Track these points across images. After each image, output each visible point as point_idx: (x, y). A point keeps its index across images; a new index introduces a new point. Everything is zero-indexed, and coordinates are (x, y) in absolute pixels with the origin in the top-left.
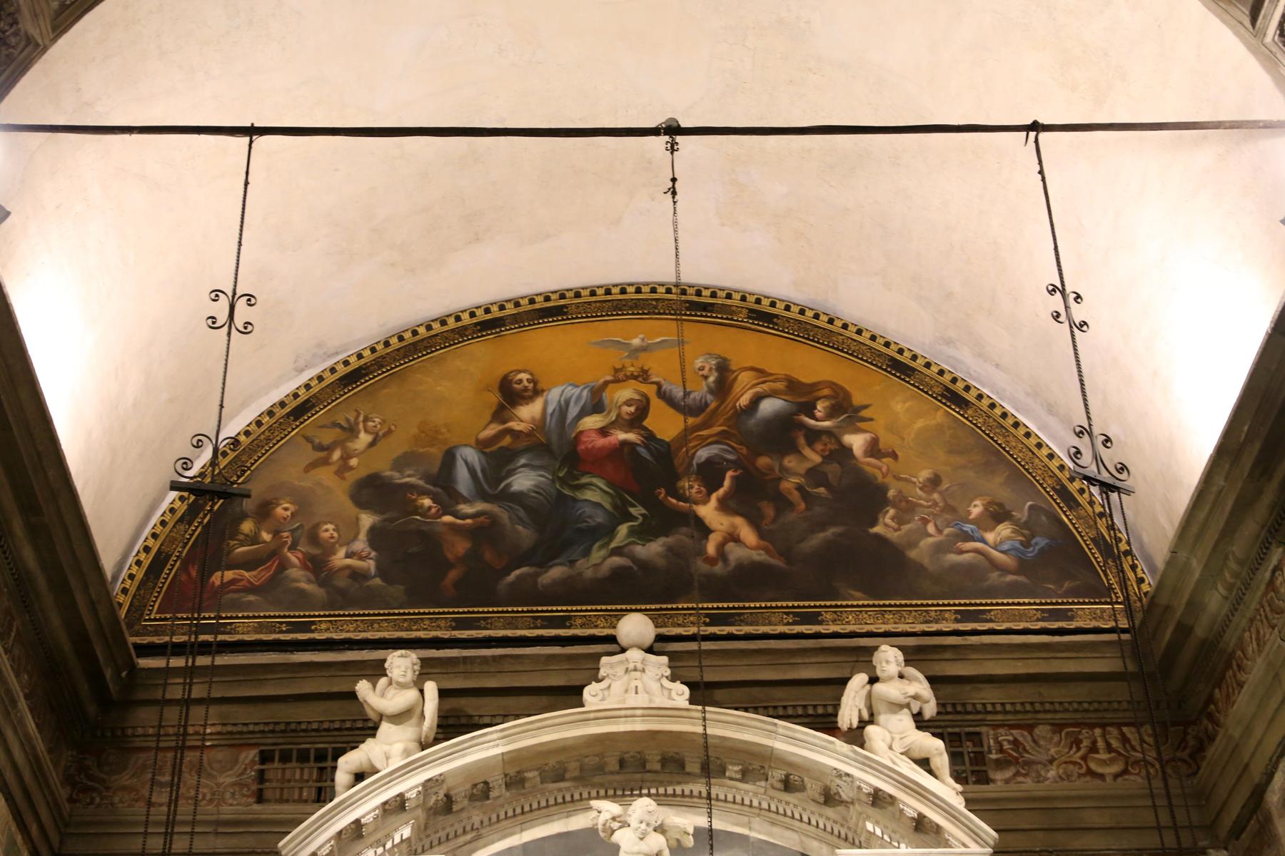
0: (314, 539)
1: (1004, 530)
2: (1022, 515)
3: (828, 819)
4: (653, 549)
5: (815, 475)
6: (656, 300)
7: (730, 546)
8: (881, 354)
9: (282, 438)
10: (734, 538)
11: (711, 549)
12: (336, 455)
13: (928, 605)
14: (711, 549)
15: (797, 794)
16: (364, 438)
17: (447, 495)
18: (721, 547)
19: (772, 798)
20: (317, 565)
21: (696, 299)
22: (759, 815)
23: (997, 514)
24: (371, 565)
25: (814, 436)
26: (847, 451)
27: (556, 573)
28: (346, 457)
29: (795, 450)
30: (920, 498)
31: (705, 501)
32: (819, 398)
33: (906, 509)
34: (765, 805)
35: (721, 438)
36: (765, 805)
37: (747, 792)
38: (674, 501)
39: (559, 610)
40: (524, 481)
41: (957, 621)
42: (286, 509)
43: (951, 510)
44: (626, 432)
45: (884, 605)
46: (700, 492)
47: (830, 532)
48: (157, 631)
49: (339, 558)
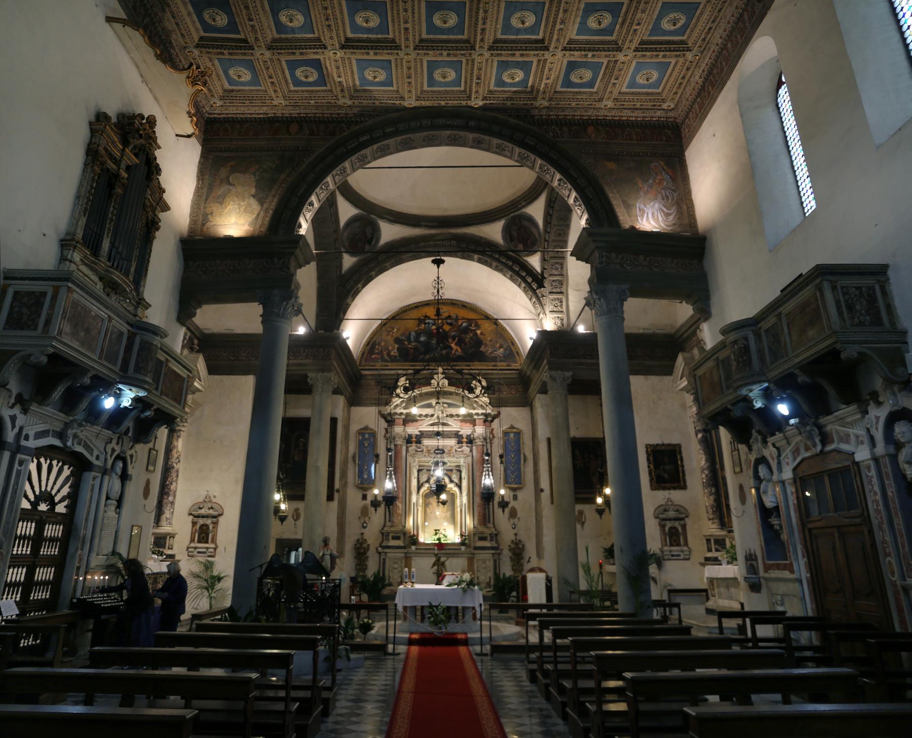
0: (388, 349)
1: (502, 350)
2: (505, 347)
4: (444, 352)
5: (471, 338)
10: (457, 350)
16: (395, 330)
17: (410, 342)
20: (389, 354)
23: (501, 347)
24: (397, 355)
25: (472, 331)
26: (477, 334)
27: (428, 357)
29: (468, 333)
33: (486, 345)
35: (456, 331)
40: (422, 339)
43: (493, 346)
47: (473, 350)
49: (392, 353)
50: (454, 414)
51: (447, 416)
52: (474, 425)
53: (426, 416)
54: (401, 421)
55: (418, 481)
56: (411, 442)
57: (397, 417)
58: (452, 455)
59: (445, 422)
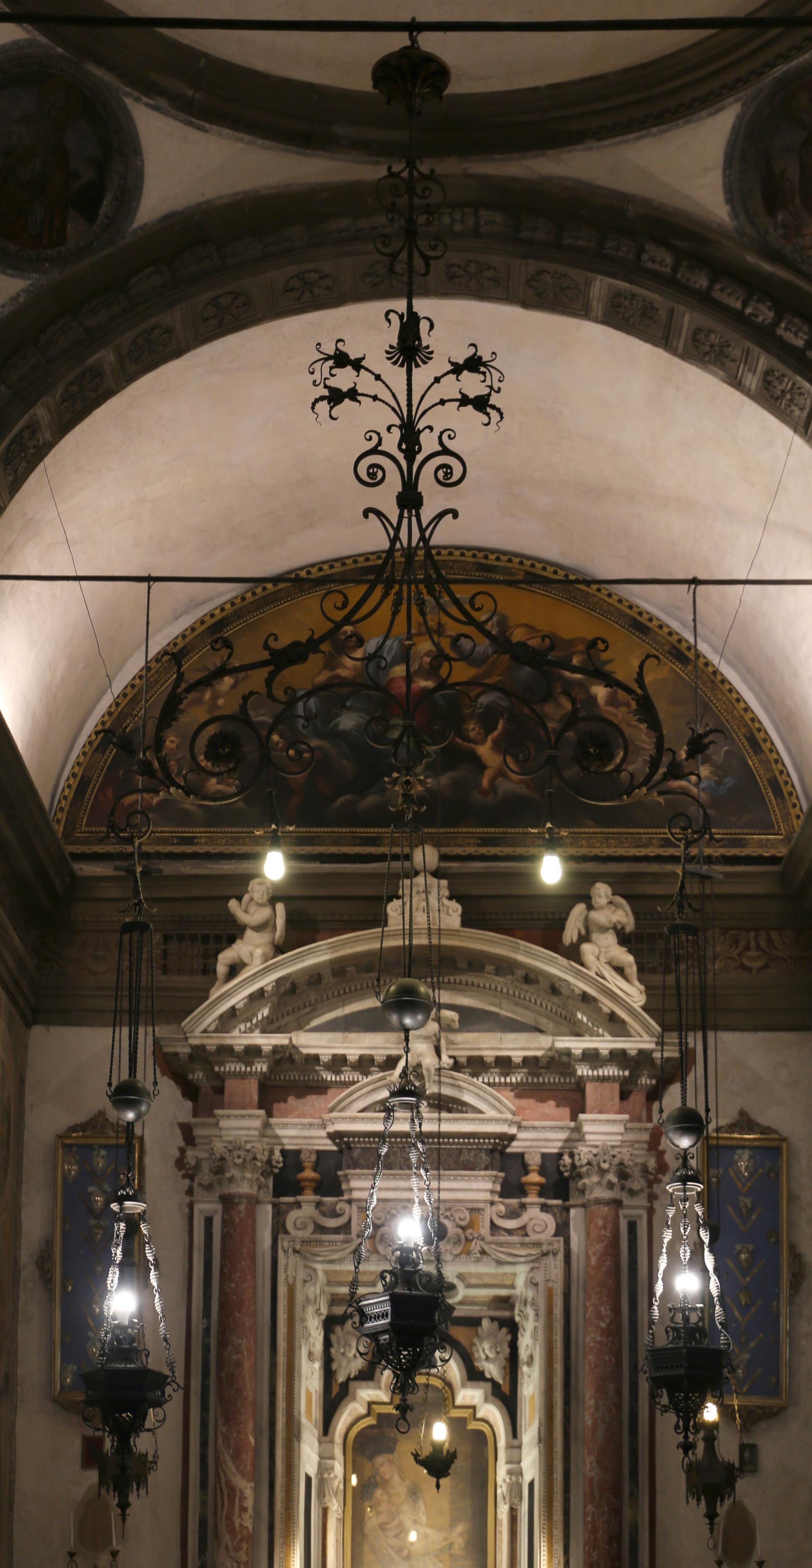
3: (554, 1003)
6: (454, 561)
7: (500, 780)
8: (625, 615)
9: (166, 681)
11: (485, 782)
12: (208, 696)
13: (640, 834)
14: (485, 782)
15: (534, 986)
18: (493, 781)
19: (516, 987)
21: (484, 561)
22: (507, 998)
27: (371, 800)
28: (214, 698)
30: (645, 742)
31: (483, 742)
32: (575, 653)
34: (511, 992)
36: (511, 992)
37: (499, 982)
38: (459, 741)
39: (373, 831)
41: (661, 846)
42: (172, 742)
44: (426, 680)
45: (609, 833)
46: (479, 734)
48: (86, 842)
50: (489, 1055)
51: (457, 1066)
52: (578, 1107)
53: (365, 1064)
54: (253, 1087)
55: (328, 1374)
56: (297, 1190)
57: (232, 1066)
58: (475, 1246)
59: (447, 1091)
